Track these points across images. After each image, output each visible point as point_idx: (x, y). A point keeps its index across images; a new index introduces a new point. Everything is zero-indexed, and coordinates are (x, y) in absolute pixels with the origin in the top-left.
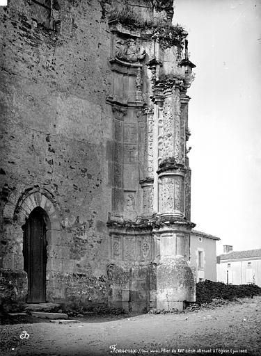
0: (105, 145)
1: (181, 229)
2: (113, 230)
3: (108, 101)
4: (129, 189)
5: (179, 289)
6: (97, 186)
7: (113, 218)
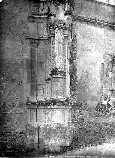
0: (25, 62)
1: (60, 107)
2: (29, 107)
3: (26, 38)
4: (40, 84)
5: (57, 140)
6: (19, 84)
7: (30, 100)
